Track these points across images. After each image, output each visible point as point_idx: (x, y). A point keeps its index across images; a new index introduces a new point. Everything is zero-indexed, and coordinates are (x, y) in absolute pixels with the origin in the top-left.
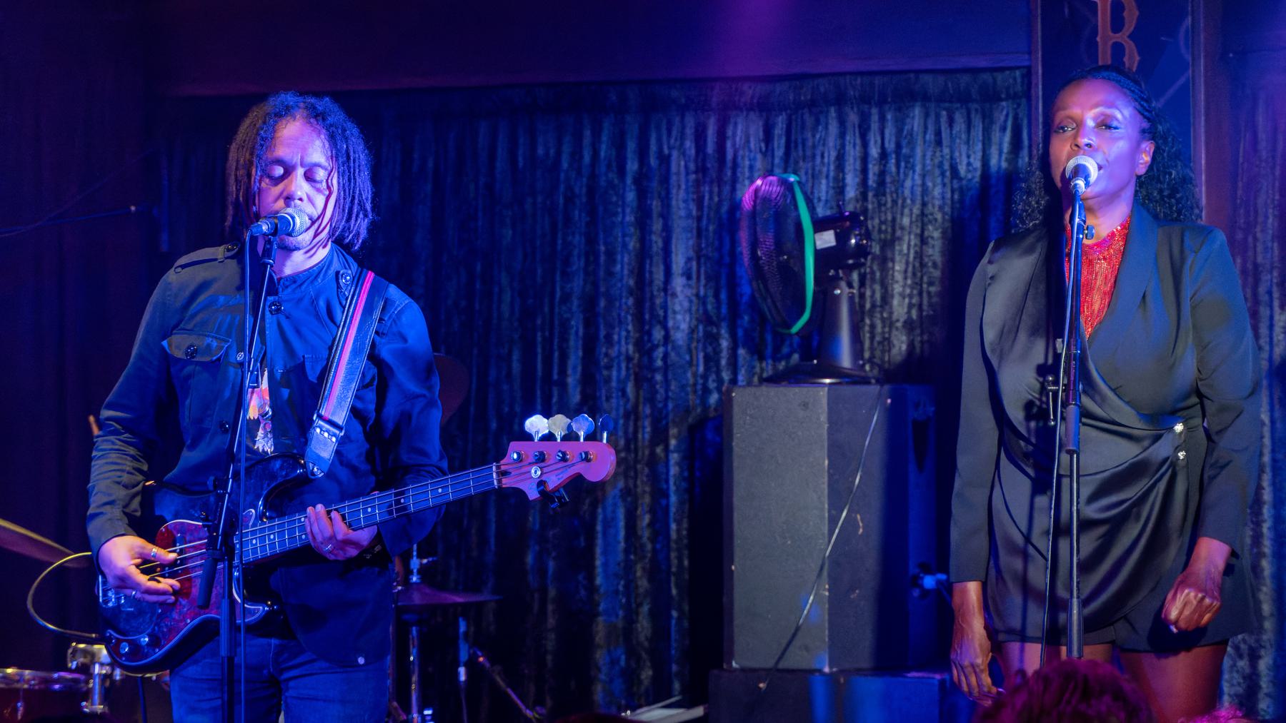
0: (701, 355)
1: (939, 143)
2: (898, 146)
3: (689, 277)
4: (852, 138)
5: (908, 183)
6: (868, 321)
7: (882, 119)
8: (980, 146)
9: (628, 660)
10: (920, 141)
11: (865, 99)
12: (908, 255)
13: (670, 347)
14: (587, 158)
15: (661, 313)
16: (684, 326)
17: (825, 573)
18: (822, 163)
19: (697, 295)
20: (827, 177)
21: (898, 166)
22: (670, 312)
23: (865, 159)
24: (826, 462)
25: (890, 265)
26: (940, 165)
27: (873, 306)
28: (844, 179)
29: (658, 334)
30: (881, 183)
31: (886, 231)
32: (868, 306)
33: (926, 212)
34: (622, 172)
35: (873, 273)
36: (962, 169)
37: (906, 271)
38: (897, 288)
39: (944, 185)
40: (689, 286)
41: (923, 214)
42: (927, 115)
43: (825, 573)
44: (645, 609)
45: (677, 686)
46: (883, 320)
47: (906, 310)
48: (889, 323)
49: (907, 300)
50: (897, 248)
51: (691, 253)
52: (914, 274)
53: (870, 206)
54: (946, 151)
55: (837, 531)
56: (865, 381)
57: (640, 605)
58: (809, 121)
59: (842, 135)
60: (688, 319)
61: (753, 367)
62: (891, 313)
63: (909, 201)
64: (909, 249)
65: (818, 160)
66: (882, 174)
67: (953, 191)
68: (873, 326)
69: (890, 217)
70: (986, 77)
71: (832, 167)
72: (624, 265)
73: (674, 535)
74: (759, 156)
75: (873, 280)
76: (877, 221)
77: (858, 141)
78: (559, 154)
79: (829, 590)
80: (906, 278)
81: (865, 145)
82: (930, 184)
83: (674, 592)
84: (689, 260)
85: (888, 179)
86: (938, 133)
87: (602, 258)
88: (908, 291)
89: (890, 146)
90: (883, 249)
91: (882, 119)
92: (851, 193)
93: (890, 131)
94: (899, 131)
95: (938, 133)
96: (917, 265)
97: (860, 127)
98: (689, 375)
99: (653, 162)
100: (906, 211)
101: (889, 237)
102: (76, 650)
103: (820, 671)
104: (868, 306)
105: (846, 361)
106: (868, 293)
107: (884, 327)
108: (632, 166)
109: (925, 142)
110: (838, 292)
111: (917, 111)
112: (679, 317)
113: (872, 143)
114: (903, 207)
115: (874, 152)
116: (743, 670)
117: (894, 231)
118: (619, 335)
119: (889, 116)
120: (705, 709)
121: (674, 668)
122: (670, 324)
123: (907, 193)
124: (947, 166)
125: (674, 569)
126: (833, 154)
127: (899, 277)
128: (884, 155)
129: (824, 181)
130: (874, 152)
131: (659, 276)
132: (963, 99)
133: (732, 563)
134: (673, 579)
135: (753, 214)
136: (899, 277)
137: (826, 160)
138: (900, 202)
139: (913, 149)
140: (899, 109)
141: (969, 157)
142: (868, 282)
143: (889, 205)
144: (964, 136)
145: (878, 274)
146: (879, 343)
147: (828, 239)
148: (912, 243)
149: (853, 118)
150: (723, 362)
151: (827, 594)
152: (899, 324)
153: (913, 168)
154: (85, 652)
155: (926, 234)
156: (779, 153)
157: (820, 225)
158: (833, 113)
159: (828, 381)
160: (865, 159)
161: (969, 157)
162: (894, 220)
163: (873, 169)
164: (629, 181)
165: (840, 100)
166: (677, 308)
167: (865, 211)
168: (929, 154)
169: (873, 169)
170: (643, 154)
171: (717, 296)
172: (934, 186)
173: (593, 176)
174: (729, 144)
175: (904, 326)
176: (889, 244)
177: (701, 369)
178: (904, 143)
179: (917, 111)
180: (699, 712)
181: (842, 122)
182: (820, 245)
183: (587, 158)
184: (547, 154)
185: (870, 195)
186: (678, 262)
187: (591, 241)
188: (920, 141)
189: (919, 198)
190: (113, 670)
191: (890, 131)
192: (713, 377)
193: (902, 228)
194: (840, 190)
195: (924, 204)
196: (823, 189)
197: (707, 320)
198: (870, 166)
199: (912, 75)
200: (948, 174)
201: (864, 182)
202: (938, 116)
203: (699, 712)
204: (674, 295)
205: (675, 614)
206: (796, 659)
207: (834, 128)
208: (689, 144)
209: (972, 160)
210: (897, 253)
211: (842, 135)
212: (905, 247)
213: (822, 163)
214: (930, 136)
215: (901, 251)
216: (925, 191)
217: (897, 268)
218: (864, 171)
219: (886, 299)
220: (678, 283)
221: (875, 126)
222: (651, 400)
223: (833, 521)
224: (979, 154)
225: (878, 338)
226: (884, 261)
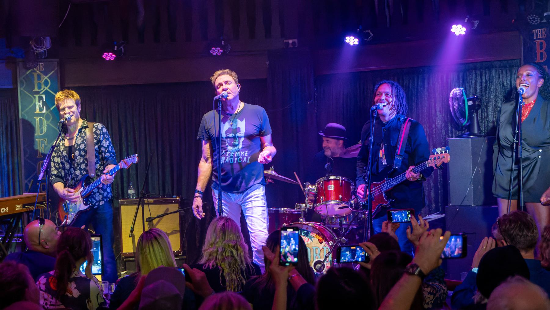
0: (444, 130)
1: (499, 78)
2: (490, 79)
3: (440, 112)
4: (479, 77)
5: (492, 88)
6: (483, 121)
7: (486, 73)
8: (509, 79)
9: (429, 203)
10: (495, 78)
11: (481, 68)
12: (492, 105)
13: (436, 129)
14: (416, 85)
15: (434, 121)
16: (440, 124)
17: (472, 183)
18: (471, 84)
19: (443, 116)
20: (473, 87)
21: (489, 84)
22: (436, 120)
23: (481, 83)
24: (471, 156)
25: (488, 107)
26: (500, 83)
27: (485, 117)
28: (476, 87)
29: (434, 126)
30: (486, 88)
31: (487, 100)
32: (483, 118)
33: (497, 95)
34: (424, 88)
35: (484, 109)
36: (505, 84)
37: (492, 109)
38: (490, 113)
39: (501, 88)
40: (441, 114)
41: (496, 95)
42: (496, 72)
43: (472, 183)
44: (433, 191)
45: (440, 208)
46: (487, 121)
47: (492, 118)
48: (488, 121)
49: (492, 116)
50: (490, 103)
51: (441, 107)
52: (494, 109)
53: (483, 94)
54: (501, 80)
55: (474, 173)
56: (480, 136)
57: (432, 190)
58: (468, 73)
59: (476, 77)
60: (440, 122)
61: (456, 133)
62: (489, 119)
63: (492, 92)
64: (493, 104)
65: (470, 83)
66: (486, 86)
67: (503, 90)
68: (485, 122)
69: (488, 96)
70: (510, 62)
71: (474, 85)
72: (425, 110)
73: (439, 173)
74: (456, 83)
75: (484, 111)
76: (485, 97)
77: (480, 78)
78: (409, 84)
79: (473, 187)
80: (492, 111)
81: (482, 79)
82: (497, 88)
83: (439, 186)
84: (440, 108)
85: (487, 87)
86: (499, 76)
87: (420, 108)
88: (493, 114)
89: (487, 79)
90: (486, 104)
91: (486, 73)
92: (478, 91)
93: (487, 75)
94: (489, 76)
95: (499, 76)
96: (495, 107)
97: (480, 75)
98: (441, 135)
99: (431, 85)
100: (492, 94)
101: (488, 101)
102: (297, 205)
103: (471, 206)
104: (483, 118)
105: (476, 132)
106: (483, 114)
107: (487, 122)
108: (426, 86)
109: (496, 78)
110: (474, 115)
111: (494, 71)
112: (438, 122)
113: (483, 79)
114: (491, 94)
115: (484, 81)
116: (453, 206)
117: (489, 100)
118: (425, 126)
119: (487, 72)
120: (445, 215)
121: (440, 204)
122: (436, 123)
123: (492, 90)
124: (501, 84)
125: (439, 181)
126: (474, 82)
127: (490, 110)
128: (486, 81)
129: (472, 88)
130: (484, 81)
131: (433, 111)
132: (505, 67)
133: (449, 180)
134: (439, 183)
135: (452, 98)
136: (490, 110)
137: (472, 83)
138: (490, 93)
139: (493, 80)
140: (490, 70)
141: (507, 81)
142: (483, 112)
143: (488, 93)
144: (505, 76)
145: (486, 110)
146: (486, 126)
147: (471, 103)
148: (493, 102)
149: (478, 72)
150: (449, 132)
151: (472, 187)
152: (491, 122)
153: (493, 84)
154: (299, 206)
155: (497, 100)
156: (461, 82)
157: (469, 100)
158: (474, 72)
159: (472, 137)
160: (481, 83)
161: (507, 81)
162: (489, 97)
163: (484, 85)
164: (426, 89)
165: (475, 69)
166: (438, 120)
167: (482, 95)
168: (497, 81)
169: (484, 85)
170: (429, 83)
171: (447, 116)
172: (498, 88)
173: (417, 89)
174: (449, 81)
175: (492, 122)
176: (488, 102)
177: (444, 134)
178: (491, 78)
179: (494, 71)
180: (443, 215)
181: (476, 74)
182: (469, 104)
183: (416, 85)
184: (406, 84)
185: (483, 91)
186: (438, 109)
187: (417, 104)
188: (495, 78)
189: (495, 91)
190: (305, 209)
191: (487, 75)
192: (447, 135)
193: (491, 99)
194: (476, 90)
195: (496, 93)
196: (472, 90)
197: (446, 123)
198: (483, 84)
199: (492, 62)
200: (502, 85)
201: (481, 88)
202: (499, 71)
203: (443, 215)
204: (437, 116)
205: (439, 192)
206: (466, 203)
207: (474, 75)
208: (440, 80)
209: (507, 82)
210: (490, 105)
211: (476, 77)
212: (492, 103)
213: (471, 84)
214: (497, 76)
215: (491, 104)
216: (496, 90)
217: (490, 108)
218: (482, 85)
219: (488, 116)
220: (438, 113)
221: (484, 75)
222: (433, 141)
223: (473, 170)
224: (509, 81)
225: (486, 125)
226: (487, 106)
